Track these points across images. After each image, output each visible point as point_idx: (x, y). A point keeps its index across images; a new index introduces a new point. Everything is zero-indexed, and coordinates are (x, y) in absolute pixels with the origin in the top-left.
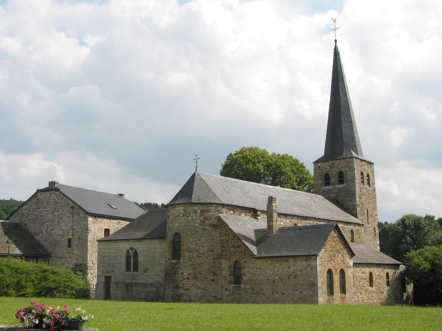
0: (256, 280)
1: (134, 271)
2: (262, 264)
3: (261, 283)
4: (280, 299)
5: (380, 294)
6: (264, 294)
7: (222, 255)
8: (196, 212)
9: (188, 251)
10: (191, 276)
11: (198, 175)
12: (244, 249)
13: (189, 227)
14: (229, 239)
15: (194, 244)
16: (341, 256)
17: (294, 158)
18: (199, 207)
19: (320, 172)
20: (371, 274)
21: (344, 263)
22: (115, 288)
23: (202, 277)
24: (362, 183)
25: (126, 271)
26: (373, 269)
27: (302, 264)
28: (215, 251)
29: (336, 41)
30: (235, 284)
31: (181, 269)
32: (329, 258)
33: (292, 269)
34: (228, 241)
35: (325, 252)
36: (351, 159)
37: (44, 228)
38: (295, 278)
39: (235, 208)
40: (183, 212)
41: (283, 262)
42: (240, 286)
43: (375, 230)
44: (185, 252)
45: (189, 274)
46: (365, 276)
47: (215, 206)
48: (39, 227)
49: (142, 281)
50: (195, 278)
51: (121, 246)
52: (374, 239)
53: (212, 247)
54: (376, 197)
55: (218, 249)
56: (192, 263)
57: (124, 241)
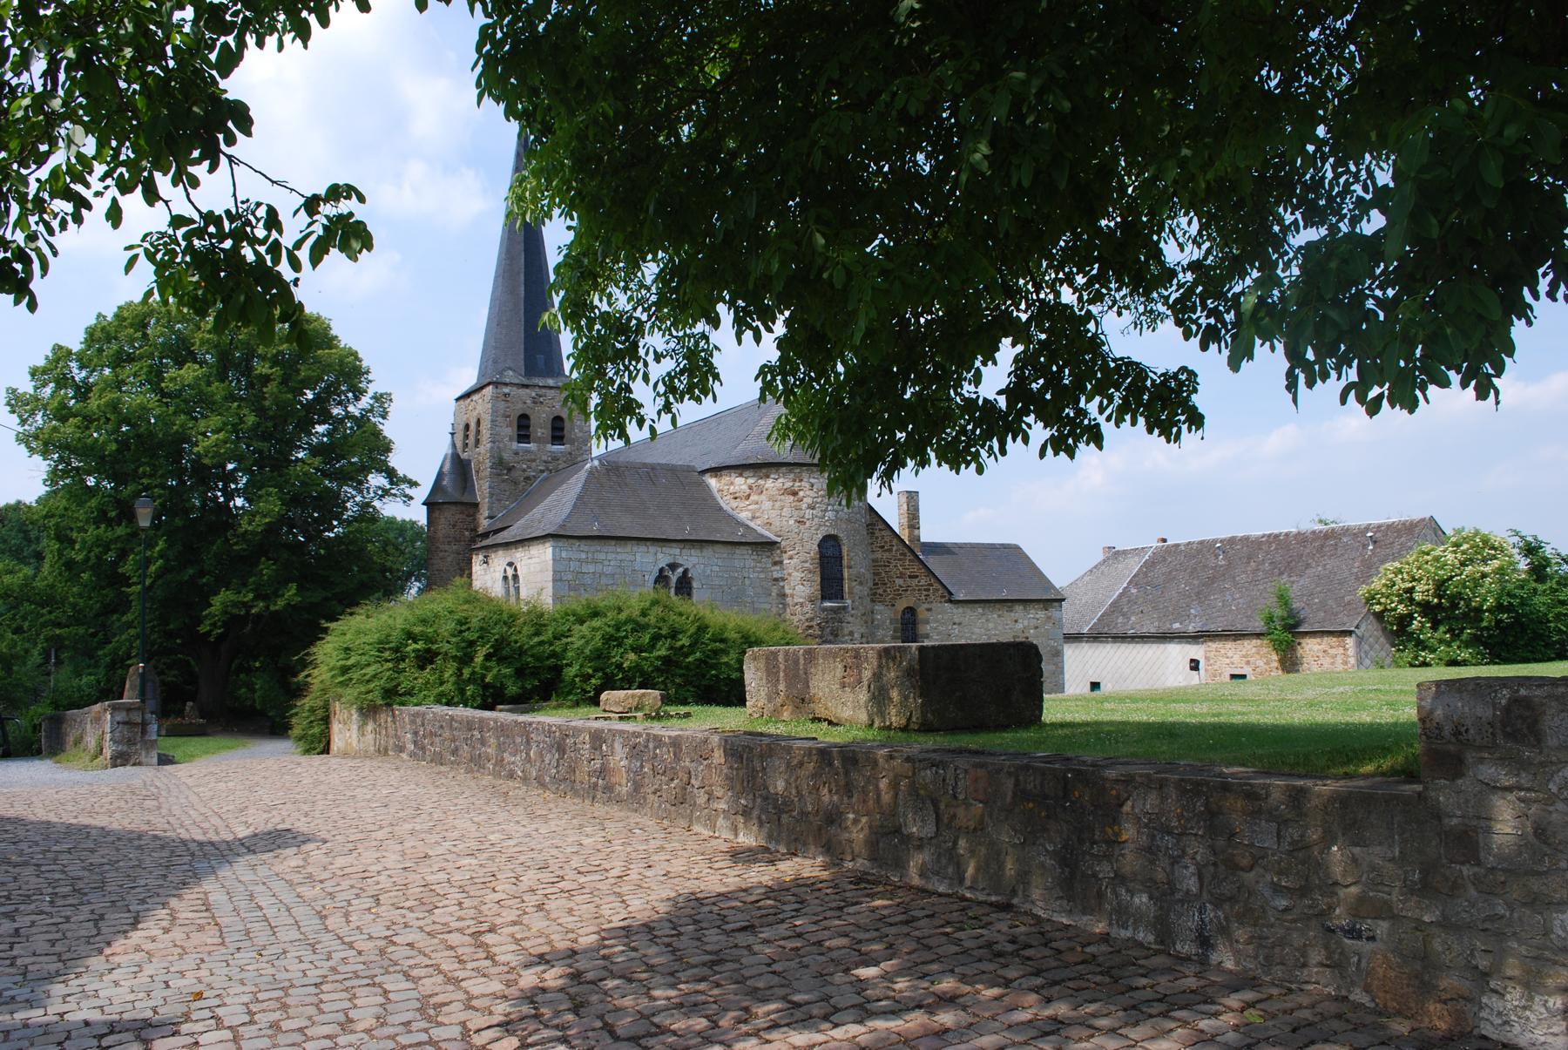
17: (1134, 423)
33: (1020, 626)
51: (638, 558)
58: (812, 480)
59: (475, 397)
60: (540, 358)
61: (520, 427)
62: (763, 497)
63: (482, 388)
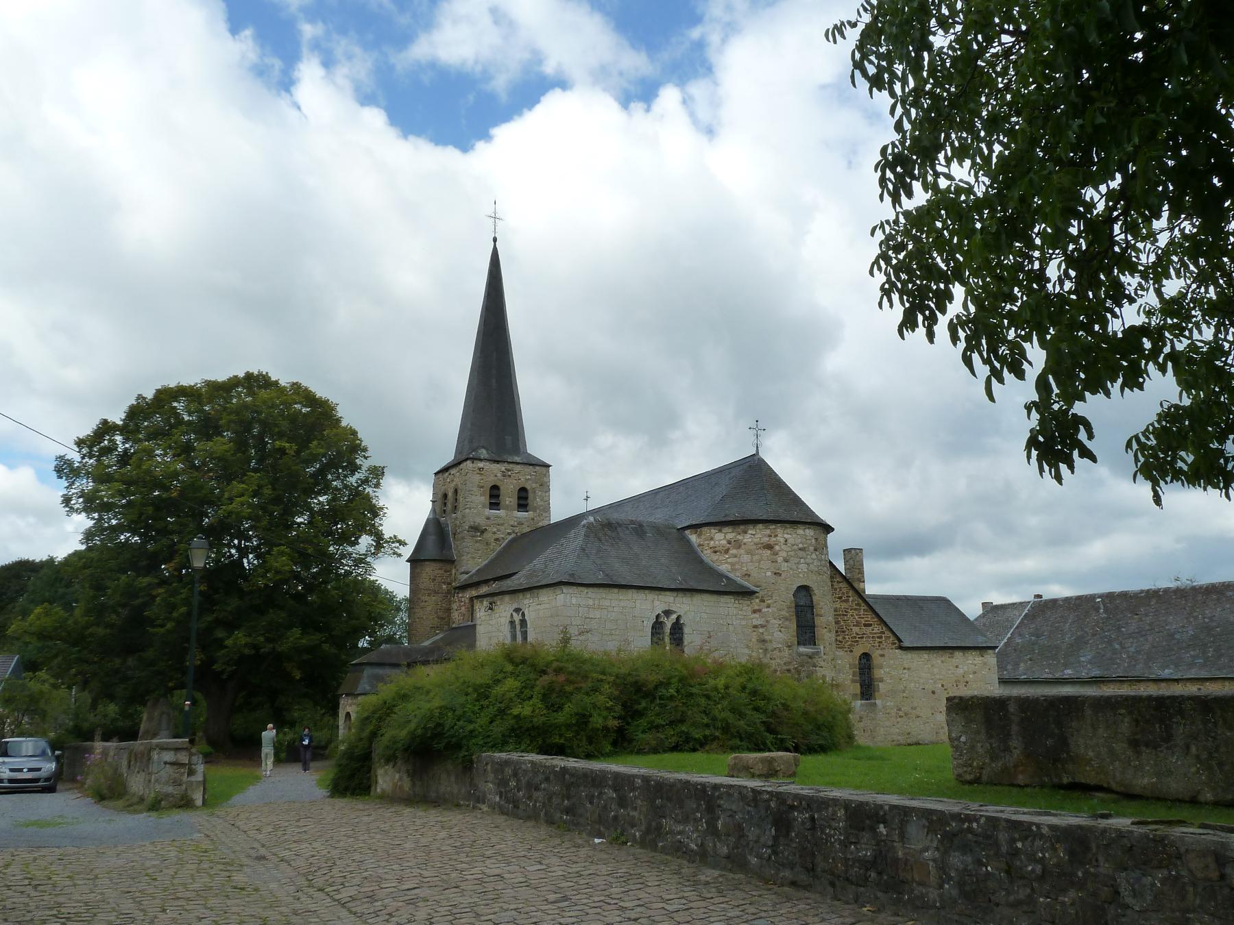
0: (904, 692)
29: (495, 240)
31: (821, 667)
33: (960, 671)
34: (846, 612)
36: (544, 469)
51: (638, 605)
57: (647, 591)
58: (786, 536)
59: (453, 471)
60: (508, 439)
61: (491, 496)
62: (742, 551)
63: (460, 463)
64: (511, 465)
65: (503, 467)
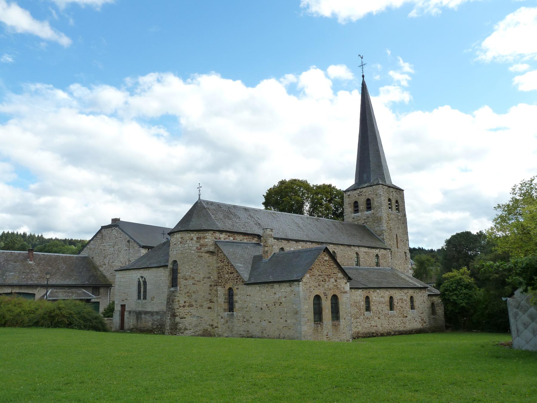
1: (143, 299)
2: (251, 291)
3: (251, 311)
4: (267, 327)
5: (403, 318)
6: (253, 322)
7: (218, 282)
8: (192, 239)
9: (184, 278)
10: (187, 304)
11: (200, 203)
12: (236, 275)
13: (186, 255)
14: (224, 266)
15: (190, 271)
16: (334, 281)
18: (195, 234)
19: (350, 200)
20: (391, 298)
21: (338, 288)
22: (128, 316)
23: (197, 305)
24: (397, 210)
25: (137, 299)
26: (392, 292)
27: (286, 290)
28: (212, 278)
29: (363, 76)
30: (230, 312)
32: (317, 284)
33: (277, 296)
34: (223, 267)
35: (311, 277)
36: (377, 186)
37: (106, 261)
38: (280, 305)
39: (235, 234)
40: (180, 239)
41: (270, 289)
42: (233, 315)
43: (406, 254)
44: (181, 280)
45: (185, 302)
46: (384, 300)
47: (212, 232)
48: (103, 260)
49: (149, 309)
50: (191, 306)
52: (405, 263)
53: (209, 274)
54: (406, 222)
55: (214, 276)
56: (187, 291)
60: (365, 176)
64: (362, 189)
65: (358, 191)
